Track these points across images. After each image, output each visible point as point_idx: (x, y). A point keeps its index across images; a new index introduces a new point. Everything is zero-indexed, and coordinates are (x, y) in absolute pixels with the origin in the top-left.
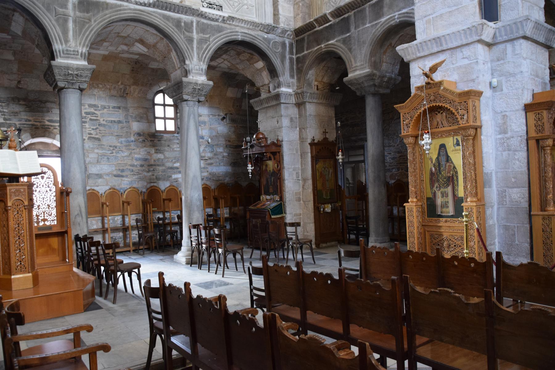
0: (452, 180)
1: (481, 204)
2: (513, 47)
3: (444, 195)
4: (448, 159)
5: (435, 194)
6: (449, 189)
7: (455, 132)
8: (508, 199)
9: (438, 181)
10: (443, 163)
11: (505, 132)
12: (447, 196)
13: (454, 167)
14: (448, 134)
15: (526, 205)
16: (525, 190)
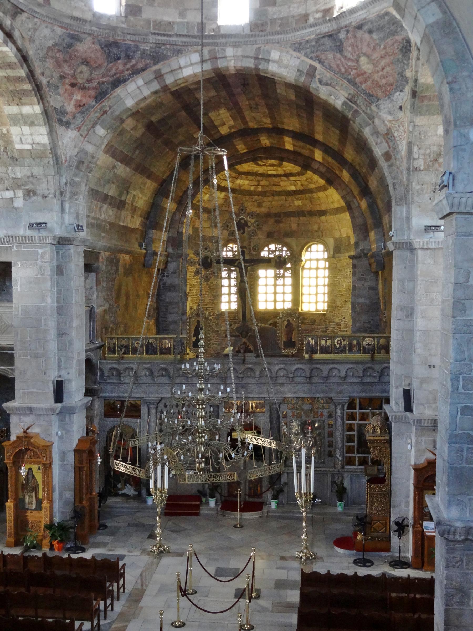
0: (35, 489)
1: (51, 502)
2: (70, 417)
3: (30, 497)
4: (33, 477)
5: (24, 497)
6: (34, 494)
7: (39, 463)
8: (64, 496)
9: (27, 489)
10: (30, 479)
11: (64, 461)
12: (32, 498)
13: (37, 482)
14: (34, 463)
15: (73, 501)
16: (73, 493)
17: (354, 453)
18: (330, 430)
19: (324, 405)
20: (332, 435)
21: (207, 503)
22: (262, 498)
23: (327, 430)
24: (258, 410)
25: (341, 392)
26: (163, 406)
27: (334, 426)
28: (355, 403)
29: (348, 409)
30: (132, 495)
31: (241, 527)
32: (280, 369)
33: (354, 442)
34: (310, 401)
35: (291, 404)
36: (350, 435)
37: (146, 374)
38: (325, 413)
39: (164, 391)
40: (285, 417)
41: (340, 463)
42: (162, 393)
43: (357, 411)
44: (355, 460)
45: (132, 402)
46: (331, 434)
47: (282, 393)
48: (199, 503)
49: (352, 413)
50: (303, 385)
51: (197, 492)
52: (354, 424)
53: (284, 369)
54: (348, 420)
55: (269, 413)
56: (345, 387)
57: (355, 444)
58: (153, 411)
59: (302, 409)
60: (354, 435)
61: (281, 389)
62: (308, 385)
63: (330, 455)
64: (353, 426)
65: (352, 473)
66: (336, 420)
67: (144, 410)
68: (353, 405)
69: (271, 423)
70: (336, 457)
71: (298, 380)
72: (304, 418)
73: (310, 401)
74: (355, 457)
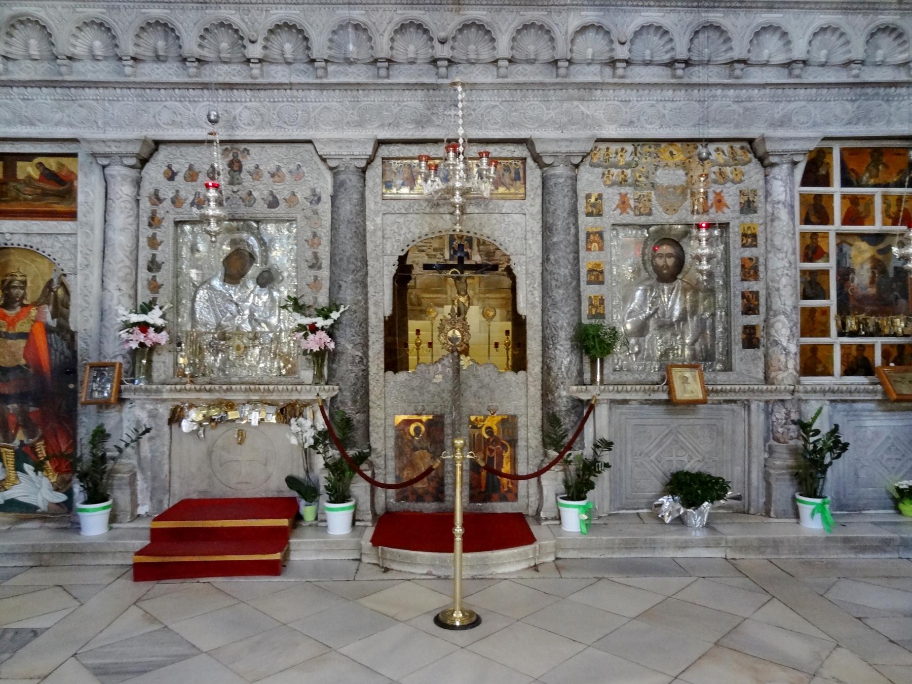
17: (826, 333)
18: (748, 253)
19: (728, 170)
20: (756, 269)
21: (320, 522)
22: (515, 497)
23: (738, 254)
24: (502, 190)
25: (783, 123)
26: (161, 178)
27: (761, 240)
28: (829, 165)
29: (804, 183)
30: (43, 506)
31: (474, 622)
32: (584, 29)
33: (825, 295)
34: (680, 157)
35: (616, 166)
36: (813, 273)
37: (91, 49)
38: (731, 195)
39: (166, 116)
40: (596, 211)
41: (791, 364)
42: (158, 126)
43: (836, 189)
44: (830, 358)
45: (52, 164)
46: (750, 270)
47: (585, 121)
48: (285, 522)
49: (818, 197)
50: (657, 94)
51: (285, 486)
52: (826, 235)
53: (599, 28)
54: (806, 221)
55: (539, 201)
56: (796, 102)
57: (832, 303)
58: (123, 191)
59: (653, 185)
60: (826, 272)
61: (583, 107)
62: (681, 93)
63: (751, 339)
64: (821, 243)
65: (839, 399)
66: (773, 218)
67: (88, 190)
68: (823, 172)
69: (547, 229)
70: (776, 343)
71: (640, 74)
72: (660, 216)
73: (680, 157)
74: (830, 346)
